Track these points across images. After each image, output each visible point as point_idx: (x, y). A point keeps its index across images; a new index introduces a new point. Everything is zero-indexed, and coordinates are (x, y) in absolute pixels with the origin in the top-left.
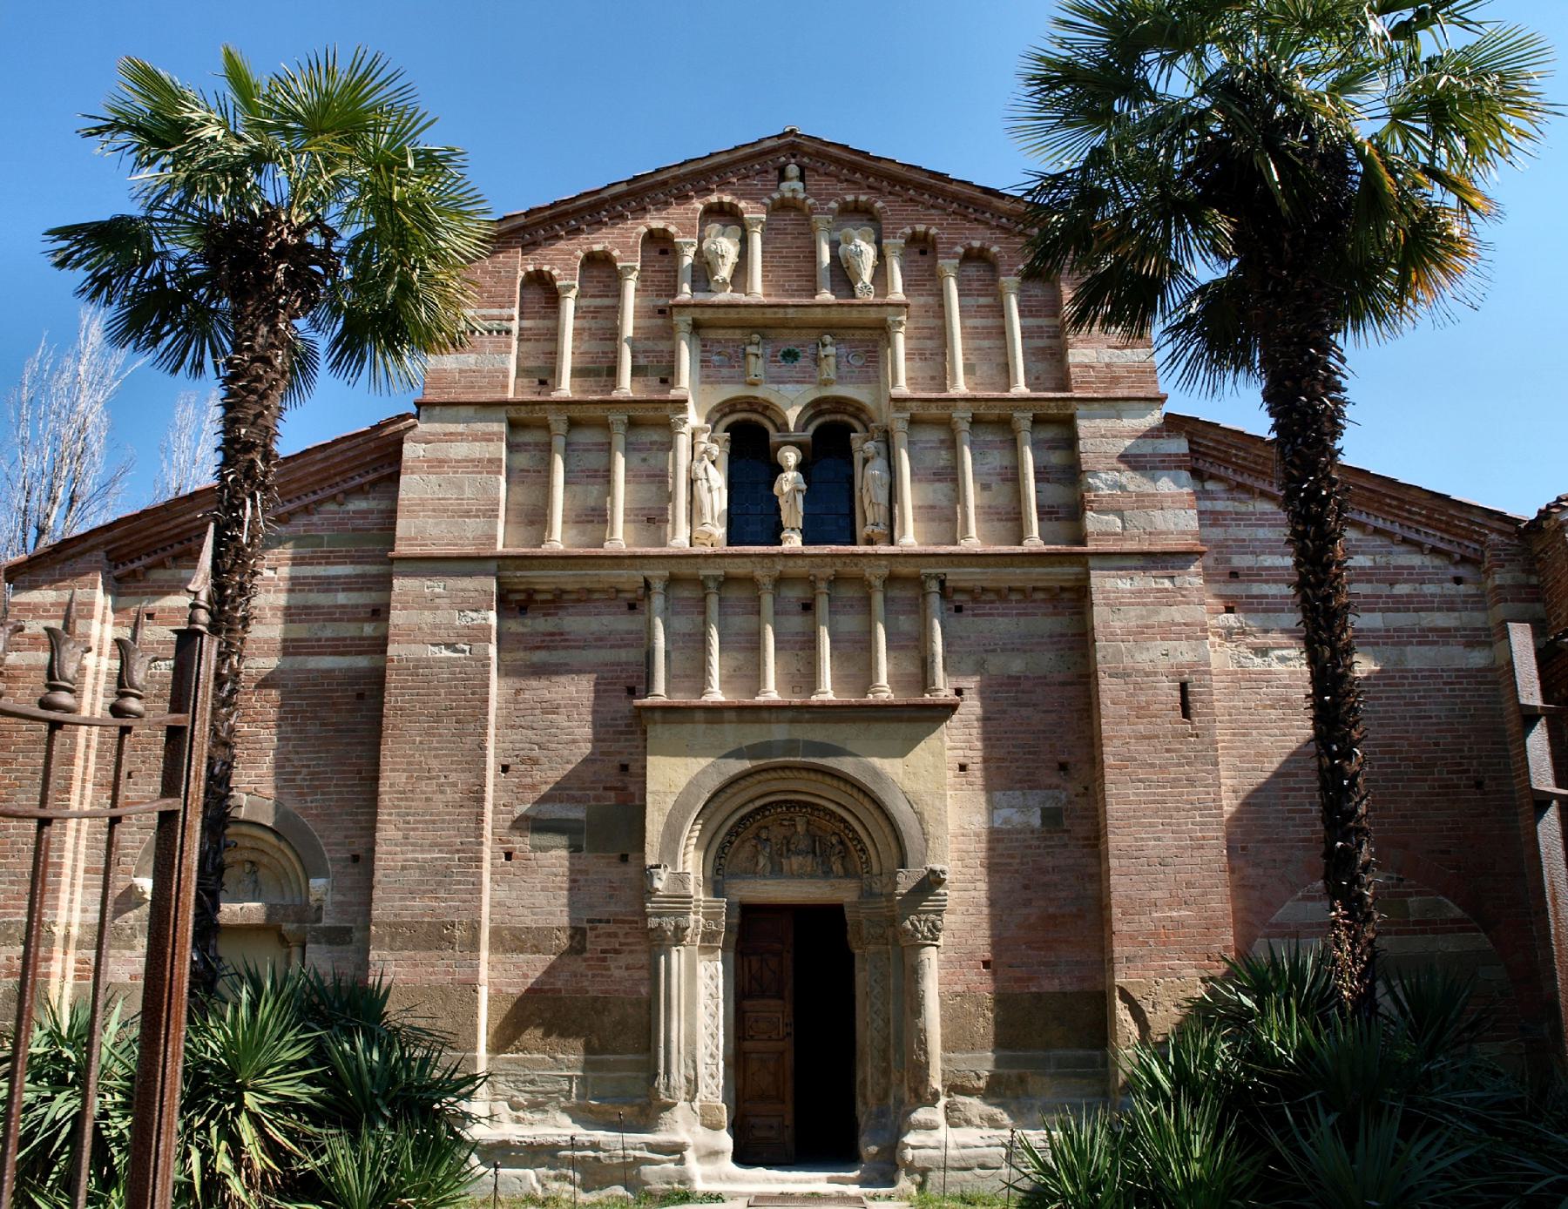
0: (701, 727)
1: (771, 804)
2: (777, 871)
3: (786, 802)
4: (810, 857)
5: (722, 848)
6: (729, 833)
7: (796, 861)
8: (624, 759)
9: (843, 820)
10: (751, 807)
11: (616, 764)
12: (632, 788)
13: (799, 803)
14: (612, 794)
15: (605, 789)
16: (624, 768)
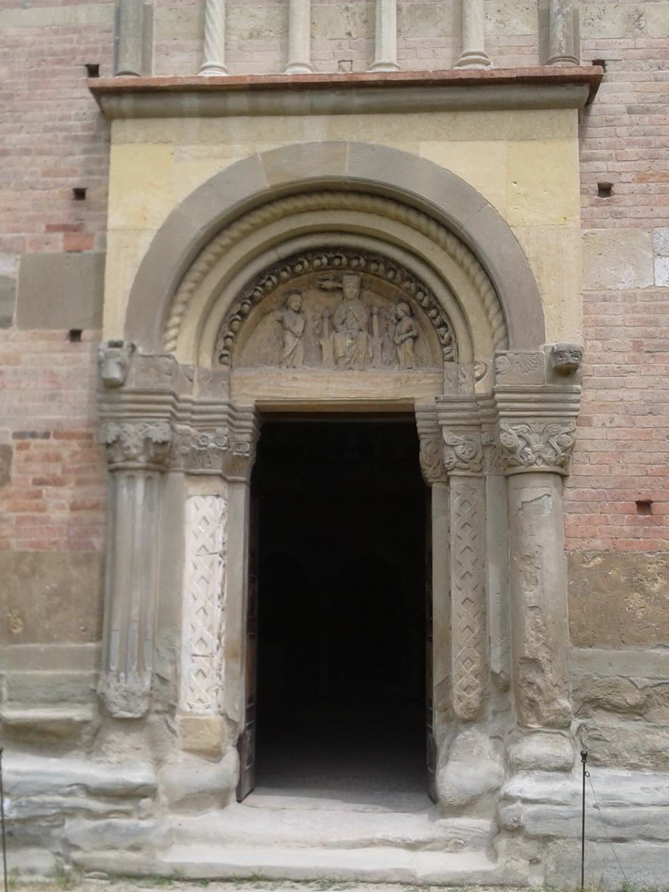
0: (193, 125)
1: (305, 253)
2: (315, 356)
3: (326, 249)
4: (364, 334)
5: (228, 320)
6: (239, 299)
7: (343, 342)
8: (76, 181)
9: (413, 277)
10: (272, 257)
11: (70, 190)
12: (91, 226)
13: (346, 250)
14: (60, 236)
15: (51, 228)
16: (80, 194)
